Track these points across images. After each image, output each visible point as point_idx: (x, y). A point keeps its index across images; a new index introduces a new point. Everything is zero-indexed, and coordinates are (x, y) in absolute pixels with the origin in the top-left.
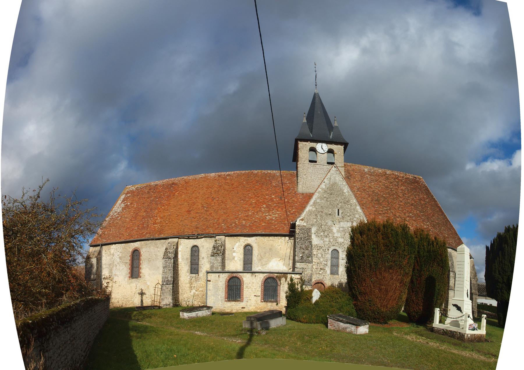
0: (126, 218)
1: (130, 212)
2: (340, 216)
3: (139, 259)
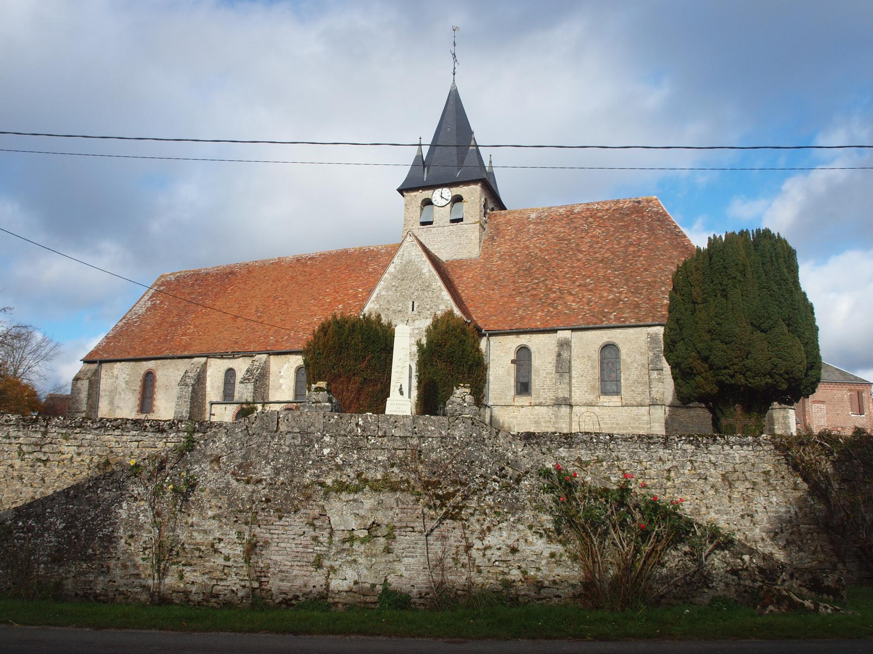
0: (148, 324)
1: (154, 315)
2: (415, 312)
3: (153, 386)
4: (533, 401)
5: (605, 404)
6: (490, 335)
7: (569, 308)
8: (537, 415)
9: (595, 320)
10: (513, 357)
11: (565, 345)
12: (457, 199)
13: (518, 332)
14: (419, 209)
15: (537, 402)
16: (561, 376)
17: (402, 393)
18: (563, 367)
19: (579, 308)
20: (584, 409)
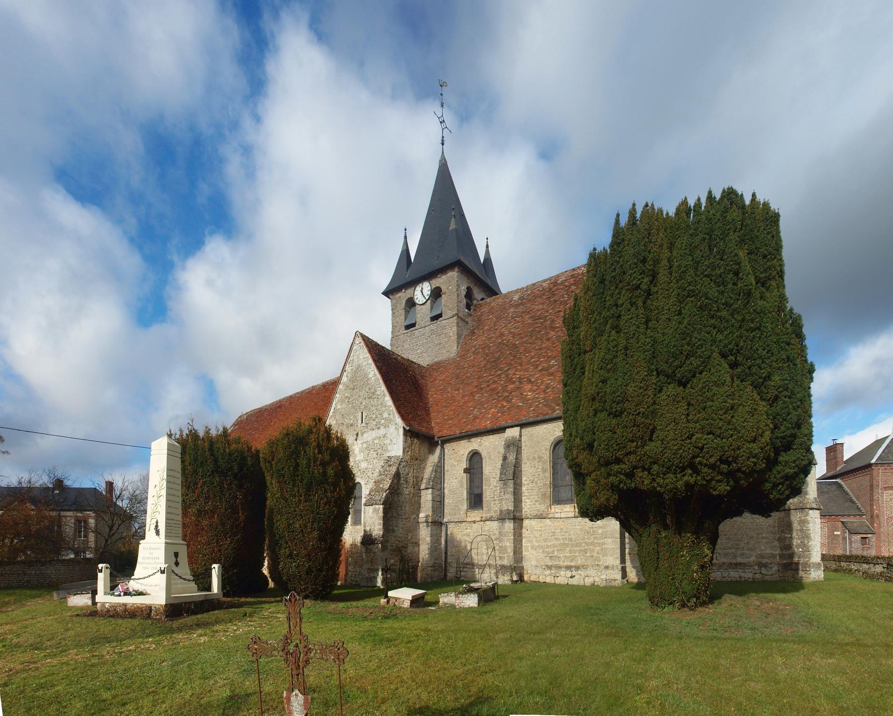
4: (484, 515)
5: (557, 515)
6: (444, 442)
7: (524, 399)
8: (489, 531)
9: (546, 410)
10: (464, 465)
11: (514, 446)
12: (436, 294)
13: (469, 436)
14: (403, 312)
15: (488, 515)
16: (505, 484)
17: (158, 533)
18: (513, 474)
19: (534, 398)
20: (534, 522)
